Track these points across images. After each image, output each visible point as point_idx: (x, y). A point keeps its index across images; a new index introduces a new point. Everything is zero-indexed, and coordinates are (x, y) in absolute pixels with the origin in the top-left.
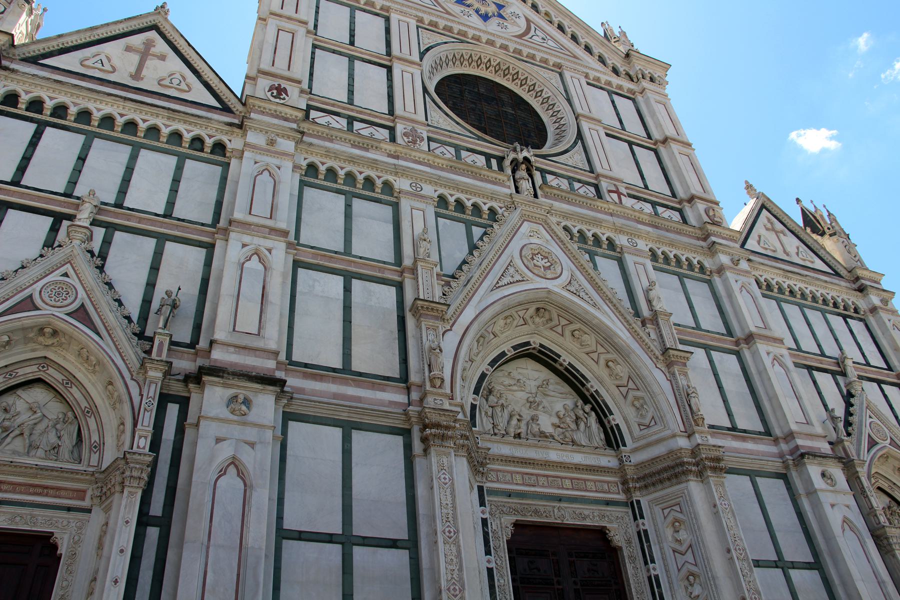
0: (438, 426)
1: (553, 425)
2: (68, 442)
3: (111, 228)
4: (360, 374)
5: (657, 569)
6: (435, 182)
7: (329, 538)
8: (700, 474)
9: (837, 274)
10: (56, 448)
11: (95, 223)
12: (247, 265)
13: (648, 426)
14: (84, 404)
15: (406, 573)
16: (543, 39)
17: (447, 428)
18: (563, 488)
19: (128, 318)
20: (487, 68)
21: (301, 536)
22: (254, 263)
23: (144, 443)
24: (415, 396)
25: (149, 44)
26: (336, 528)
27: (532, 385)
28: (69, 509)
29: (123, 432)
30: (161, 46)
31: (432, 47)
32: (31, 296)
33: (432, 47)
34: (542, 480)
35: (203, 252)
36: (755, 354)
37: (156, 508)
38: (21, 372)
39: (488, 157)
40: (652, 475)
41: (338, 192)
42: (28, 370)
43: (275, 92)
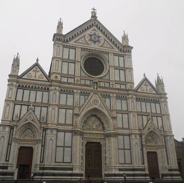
0: (76, 132)
1: (96, 127)
3: (35, 106)
4: (67, 124)
5: (106, 149)
6: (80, 89)
7: (62, 147)
8: (113, 136)
9: (158, 94)
10: (32, 137)
13: (109, 128)
15: (71, 150)
16: (107, 45)
17: (77, 132)
18: (94, 137)
19: (38, 120)
20: (94, 55)
21: (59, 146)
22: (53, 110)
24: (74, 127)
25: (36, 69)
26: (63, 145)
27: (93, 120)
29: (39, 135)
30: (38, 69)
31: (83, 55)
32: (27, 119)
33: (83, 55)
34: (92, 136)
36: (130, 115)
39: (90, 80)
40: (108, 135)
42: (27, 127)
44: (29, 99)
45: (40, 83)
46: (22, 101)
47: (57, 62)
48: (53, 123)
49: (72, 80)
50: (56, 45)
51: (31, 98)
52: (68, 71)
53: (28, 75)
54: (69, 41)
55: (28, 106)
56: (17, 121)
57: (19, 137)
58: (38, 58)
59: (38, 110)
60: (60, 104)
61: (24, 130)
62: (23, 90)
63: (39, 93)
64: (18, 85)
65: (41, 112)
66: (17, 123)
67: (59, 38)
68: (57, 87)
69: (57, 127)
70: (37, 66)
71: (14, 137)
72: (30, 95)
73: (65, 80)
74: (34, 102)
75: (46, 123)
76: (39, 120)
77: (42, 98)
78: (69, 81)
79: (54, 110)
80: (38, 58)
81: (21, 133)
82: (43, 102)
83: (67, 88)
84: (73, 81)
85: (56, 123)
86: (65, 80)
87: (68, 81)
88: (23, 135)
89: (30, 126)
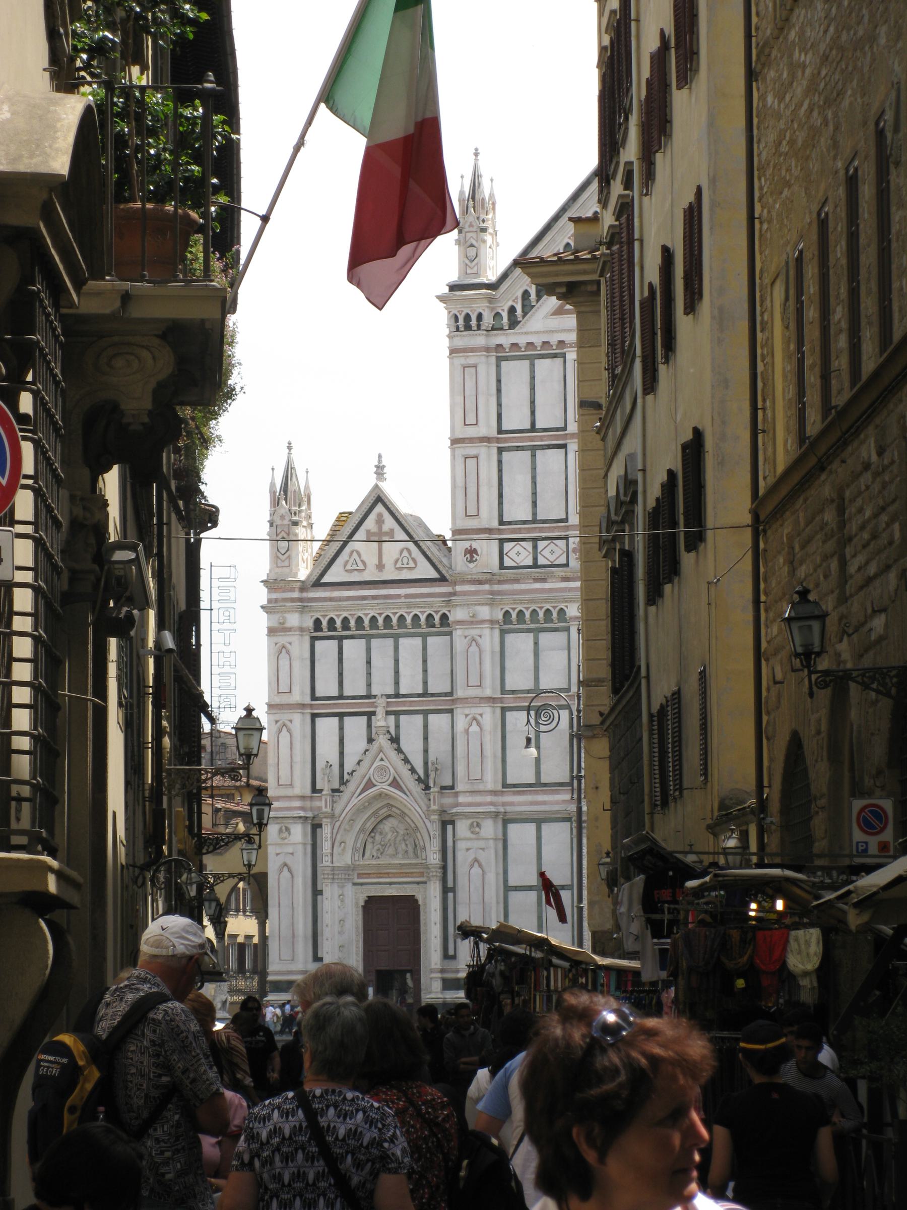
2: (410, 849)
4: (545, 785)
10: (406, 852)
11: (388, 713)
12: (470, 730)
14: (413, 825)
21: (517, 888)
22: (474, 728)
23: (434, 858)
25: (380, 521)
28: (418, 883)
30: (389, 523)
32: (370, 778)
35: (450, 715)
37: (450, 884)
38: (381, 812)
41: (528, 631)
43: (468, 556)
44: (369, 685)
45: (407, 596)
46: (341, 697)
47: (471, 463)
48: (476, 788)
49: (558, 552)
50: (460, 360)
51: (374, 680)
52: (534, 504)
53: (347, 562)
54: (525, 314)
55: (370, 715)
56: (334, 791)
57: (357, 858)
58: (380, 456)
59: (411, 727)
60: (508, 688)
61: (369, 826)
62: (335, 643)
63: (410, 646)
64: (310, 623)
65: (426, 738)
66: (333, 802)
67: (467, 318)
68: (478, 608)
69: (504, 804)
70: (380, 508)
71: (329, 864)
72: (369, 662)
73: (519, 554)
74: (391, 691)
75: (452, 787)
76: (422, 776)
77: (425, 671)
78: (541, 561)
79: (479, 724)
80: (380, 456)
81: (360, 841)
82: (431, 690)
83: (532, 601)
84: (565, 555)
85: (490, 786)
86: (524, 553)
87: (535, 559)
88: (369, 847)
89: (392, 806)
